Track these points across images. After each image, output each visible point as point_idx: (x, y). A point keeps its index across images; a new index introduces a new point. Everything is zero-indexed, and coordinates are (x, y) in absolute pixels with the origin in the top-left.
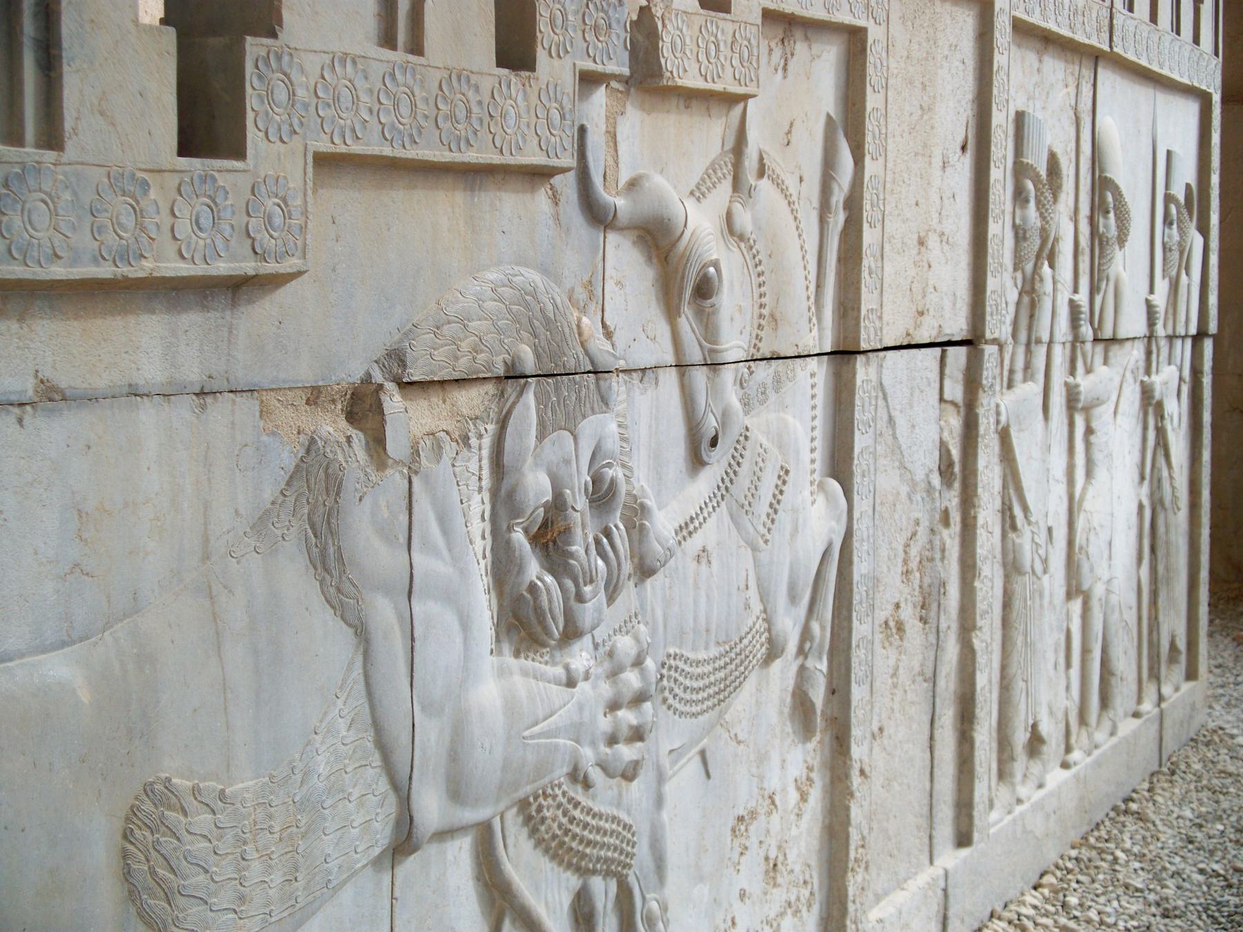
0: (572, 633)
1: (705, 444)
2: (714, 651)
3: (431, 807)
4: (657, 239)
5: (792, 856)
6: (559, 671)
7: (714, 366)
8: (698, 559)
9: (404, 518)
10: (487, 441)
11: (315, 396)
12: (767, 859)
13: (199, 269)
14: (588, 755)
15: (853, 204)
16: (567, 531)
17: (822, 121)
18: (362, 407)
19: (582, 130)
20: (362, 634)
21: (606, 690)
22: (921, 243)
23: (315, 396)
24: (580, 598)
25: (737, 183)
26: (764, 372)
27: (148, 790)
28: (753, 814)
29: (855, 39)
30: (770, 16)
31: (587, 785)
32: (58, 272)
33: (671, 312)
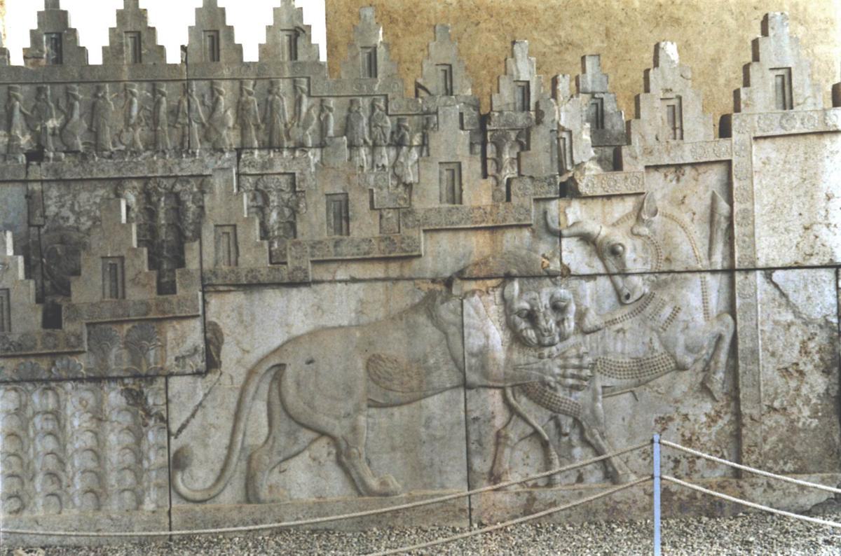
0: (541, 345)
1: (623, 298)
2: (627, 360)
3: (473, 377)
4: (586, 239)
5: (703, 440)
6: (537, 354)
7: (625, 274)
8: (618, 331)
9: (459, 309)
10: (498, 292)
11: (434, 281)
12: (683, 436)
13: (387, 255)
14: (549, 378)
15: (730, 219)
16: (537, 317)
17: (709, 193)
18: (448, 283)
19: (545, 213)
20: (446, 334)
21: (559, 362)
22: (806, 229)
23: (434, 281)
24: (543, 336)
25: (639, 219)
26: (664, 277)
27: (374, 355)
28: (671, 419)
29: (729, 162)
30: (647, 167)
31: (551, 388)
32: (349, 257)
33: (602, 259)
